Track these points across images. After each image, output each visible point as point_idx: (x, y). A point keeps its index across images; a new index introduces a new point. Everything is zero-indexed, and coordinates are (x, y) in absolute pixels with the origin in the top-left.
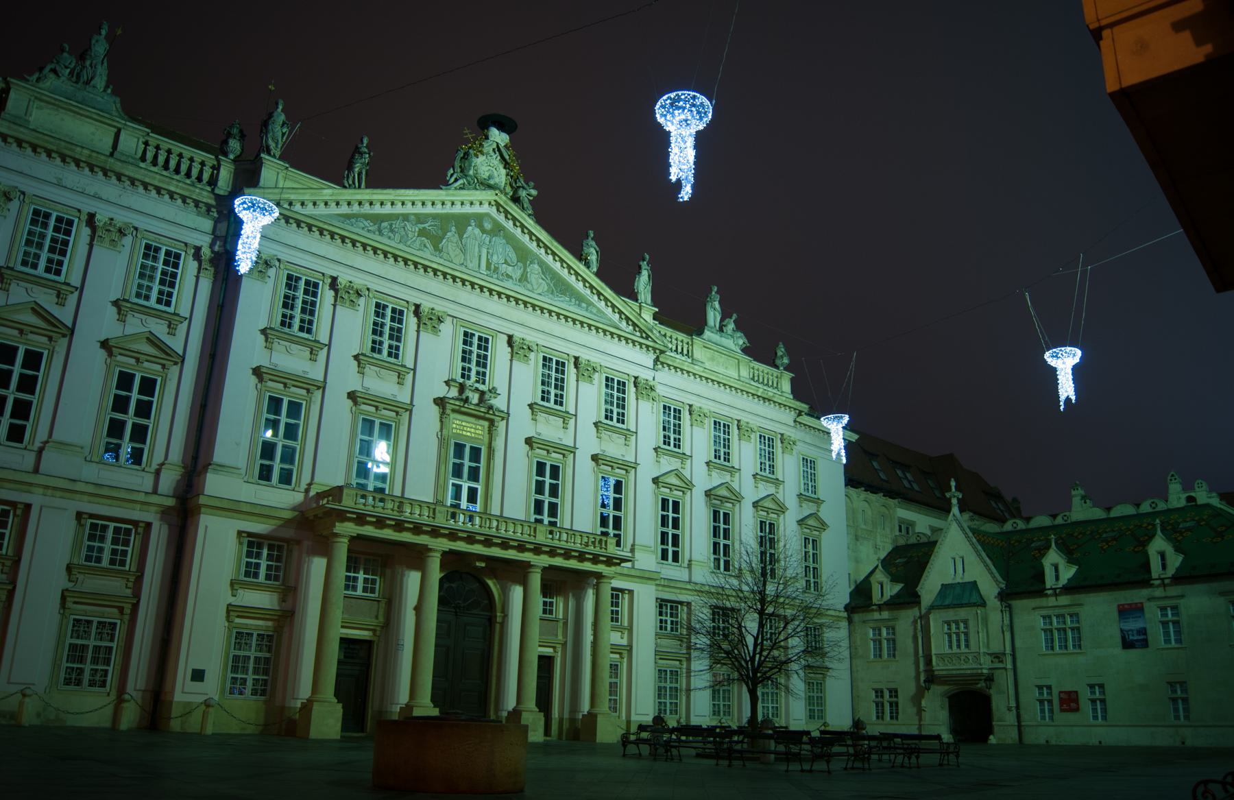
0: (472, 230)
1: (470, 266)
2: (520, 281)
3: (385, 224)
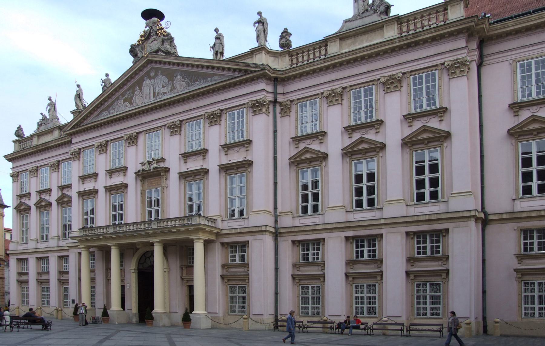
0: (147, 82)
1: (146, 101)
2: (171, 91)
3: (111, 108)
